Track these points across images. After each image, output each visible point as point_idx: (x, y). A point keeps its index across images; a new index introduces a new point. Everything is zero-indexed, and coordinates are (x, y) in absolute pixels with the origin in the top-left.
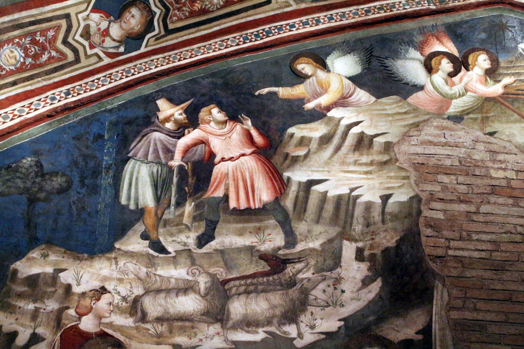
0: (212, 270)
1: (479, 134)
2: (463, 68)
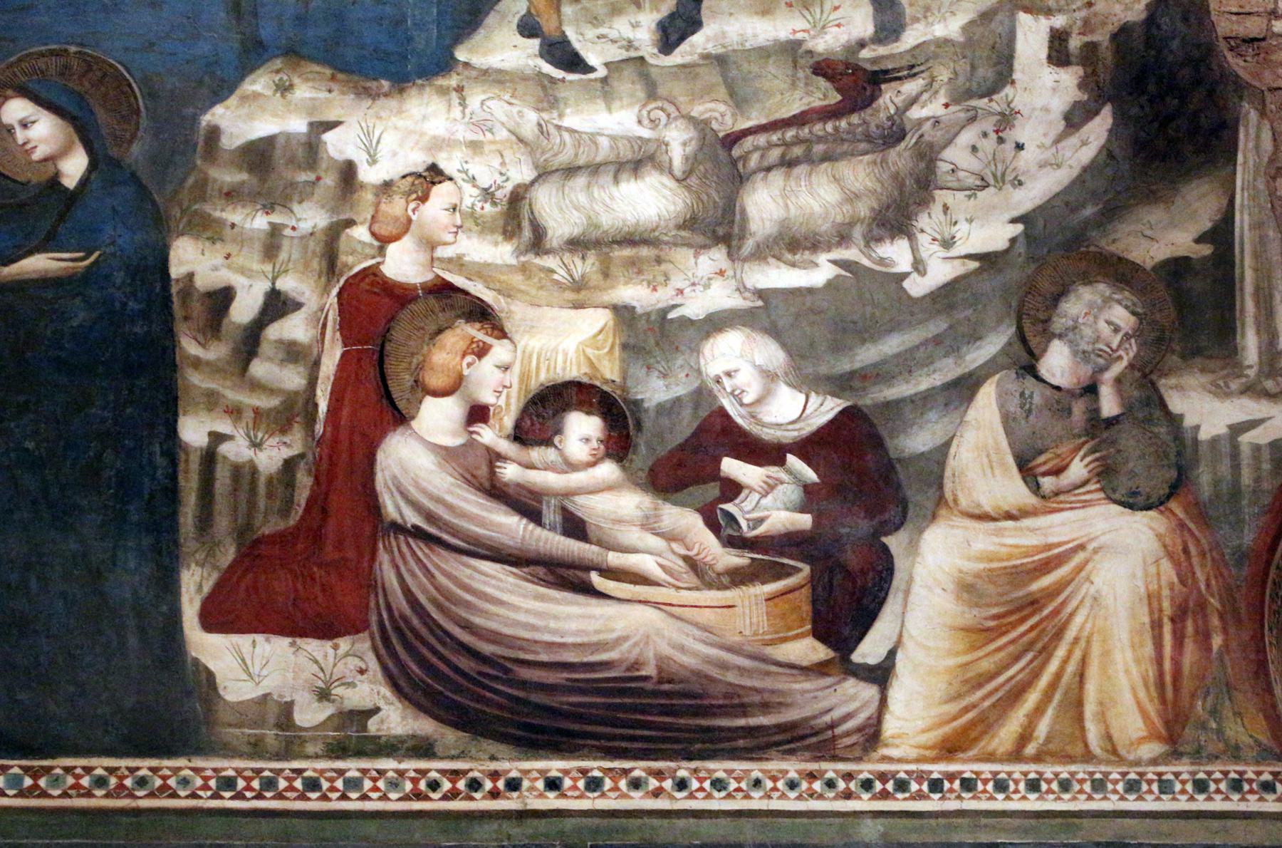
0: (698, 110)
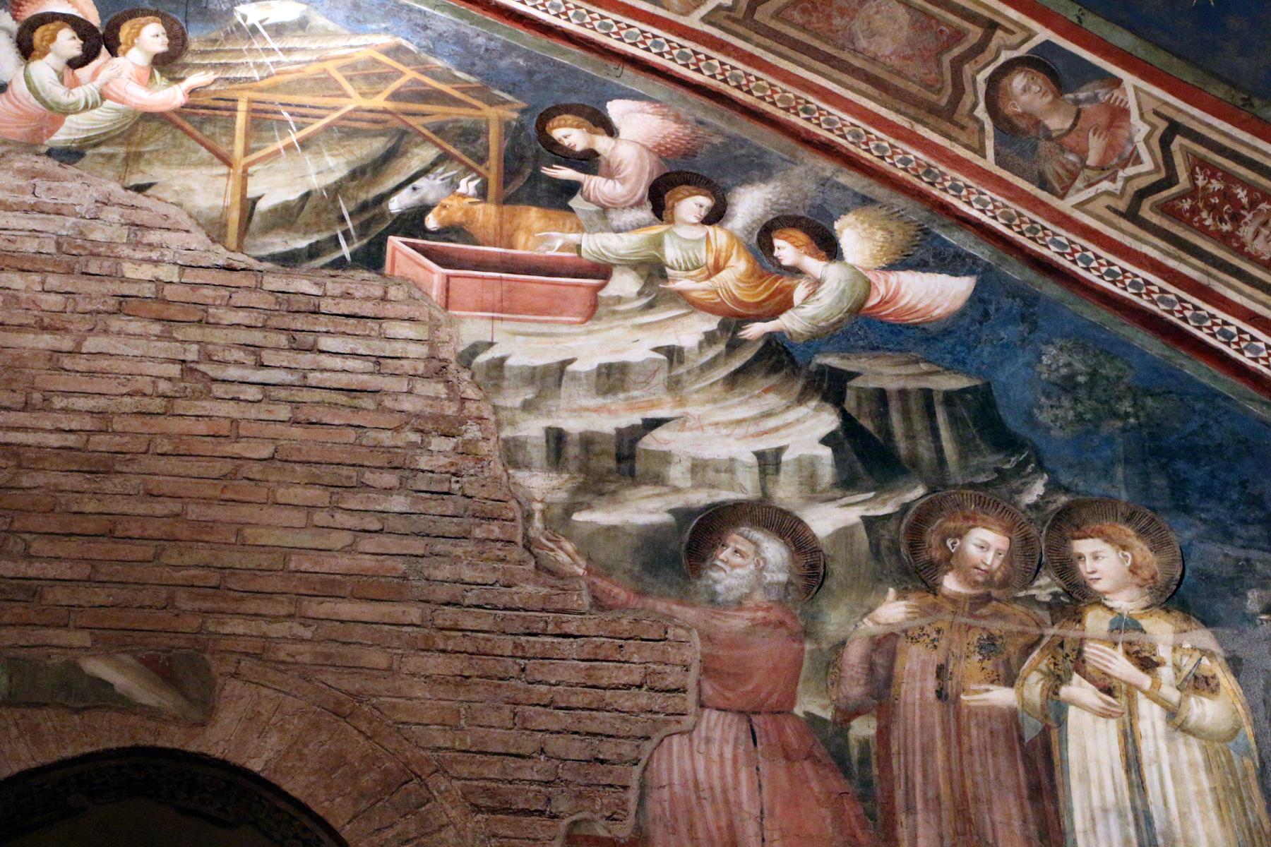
1: (114, 188)
2: (104, 49)
